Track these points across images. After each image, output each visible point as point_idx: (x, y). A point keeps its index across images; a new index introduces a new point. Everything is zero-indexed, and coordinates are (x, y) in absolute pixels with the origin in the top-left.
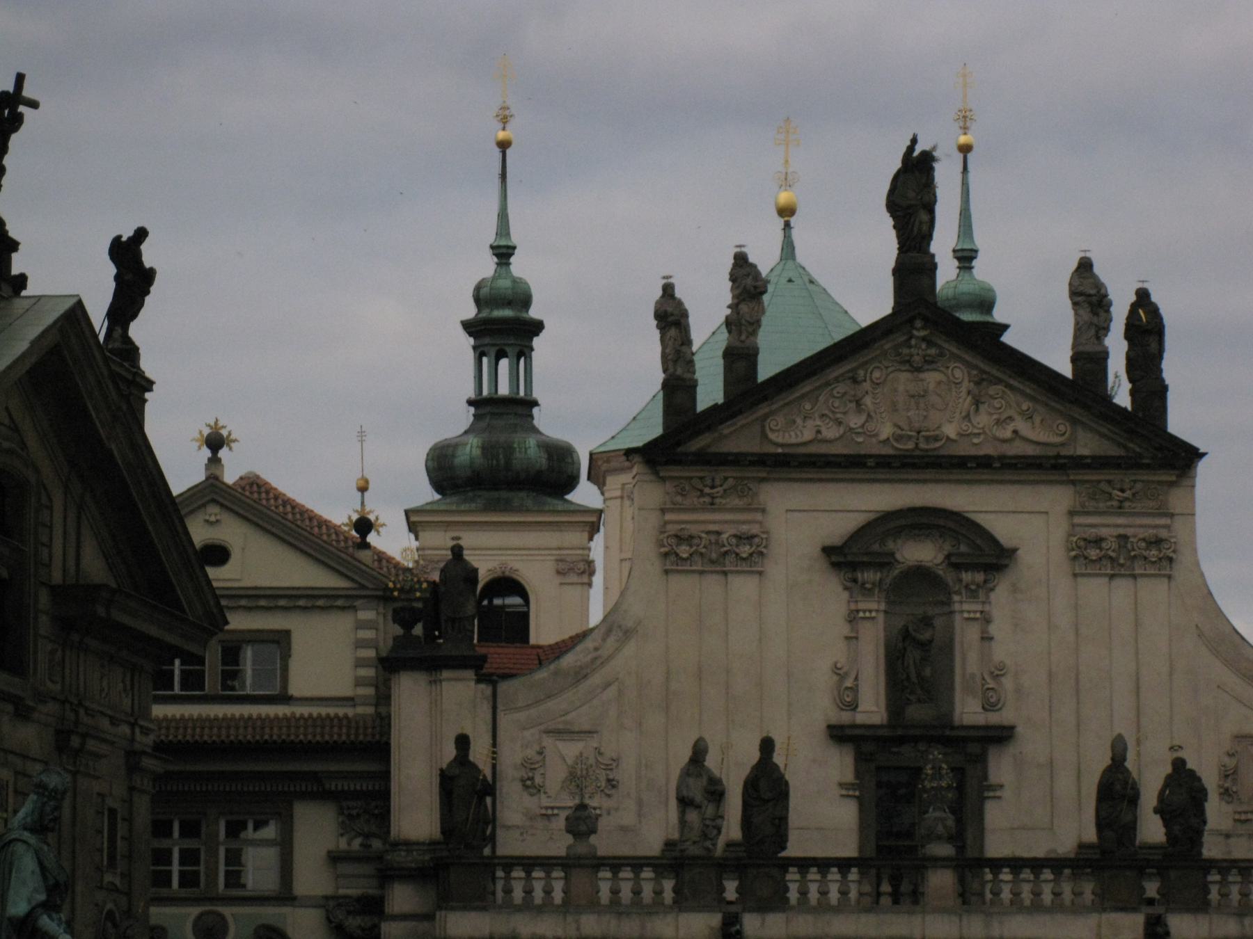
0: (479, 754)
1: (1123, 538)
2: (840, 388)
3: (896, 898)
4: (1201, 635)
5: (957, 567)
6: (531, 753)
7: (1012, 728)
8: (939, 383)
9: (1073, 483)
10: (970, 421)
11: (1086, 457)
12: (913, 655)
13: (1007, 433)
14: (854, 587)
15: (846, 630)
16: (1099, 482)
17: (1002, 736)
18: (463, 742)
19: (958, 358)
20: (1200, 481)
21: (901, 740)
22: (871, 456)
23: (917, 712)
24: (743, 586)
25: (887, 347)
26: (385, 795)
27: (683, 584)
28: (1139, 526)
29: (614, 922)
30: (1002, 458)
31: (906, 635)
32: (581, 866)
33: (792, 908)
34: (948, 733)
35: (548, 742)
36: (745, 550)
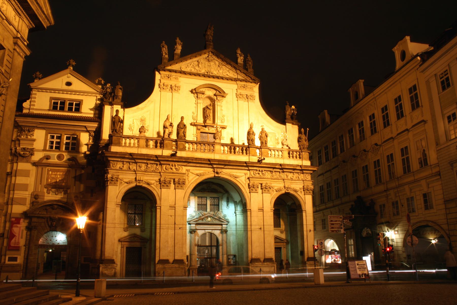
0: (121, 115)
2: (195, 63)
7: (227, 126)
8: (213, 64)
11: (240, 79)
12: (208, 111)
13: (225, 74)
17: (224, 128)
21: (205, 126)
22: (201, 74)
30: (225, 77)
31: (207, 107)
33: (187, 151)
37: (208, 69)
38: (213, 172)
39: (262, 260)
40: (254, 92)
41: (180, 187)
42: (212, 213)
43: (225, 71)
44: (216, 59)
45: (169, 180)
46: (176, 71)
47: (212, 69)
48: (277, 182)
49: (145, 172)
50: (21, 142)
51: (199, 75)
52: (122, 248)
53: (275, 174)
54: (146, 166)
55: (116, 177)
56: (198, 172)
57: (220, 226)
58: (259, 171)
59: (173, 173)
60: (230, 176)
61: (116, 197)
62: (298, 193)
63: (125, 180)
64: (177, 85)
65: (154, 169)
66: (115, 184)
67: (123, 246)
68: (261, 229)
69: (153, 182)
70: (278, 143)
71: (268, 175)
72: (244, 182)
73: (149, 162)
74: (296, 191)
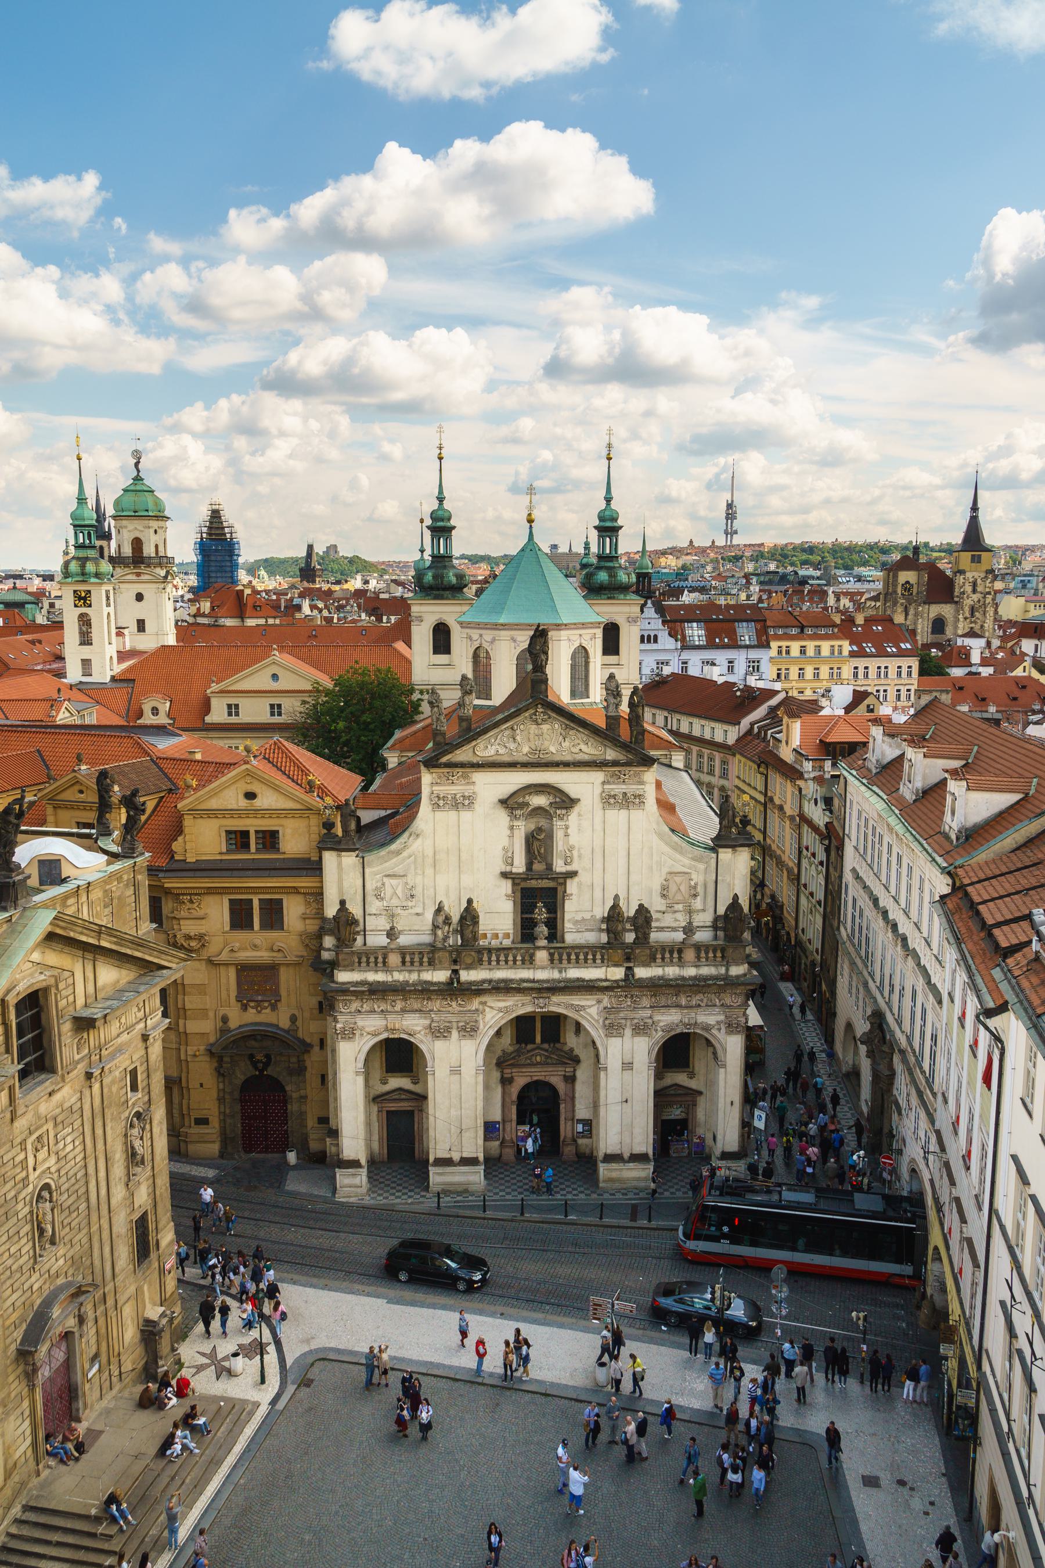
1: (625, 794)
2: (507, 733)
3: (523, 961)
6: (379, 884)
14: (513, 817)
15: (509, 832)
17: (573, 874)
18: (343, 903)
23: (538, 867)
24: (466, 815)
26: (322, 894)
27: (439, 815)
28: (631, 788)
29: (407, 975)
35: (385, 880)
36: (467, 802)
39: (626, 1156)
40: (642, 783)
42: (546, 1046)
43: (577, 741)
44: (553, 715)
46: (462, 765)
47: (546, 743)
50: (182, 922)
51: (512, 765)
56: (502, 1004)
62: (714, 1031)
63: (367, 1029)
64: (466, 794)
68: (626, 1101)
69: (419, 1028)
70: (695, 896)
71: (646, 1002)
72: (596, 1017)
74: (707, 1028)
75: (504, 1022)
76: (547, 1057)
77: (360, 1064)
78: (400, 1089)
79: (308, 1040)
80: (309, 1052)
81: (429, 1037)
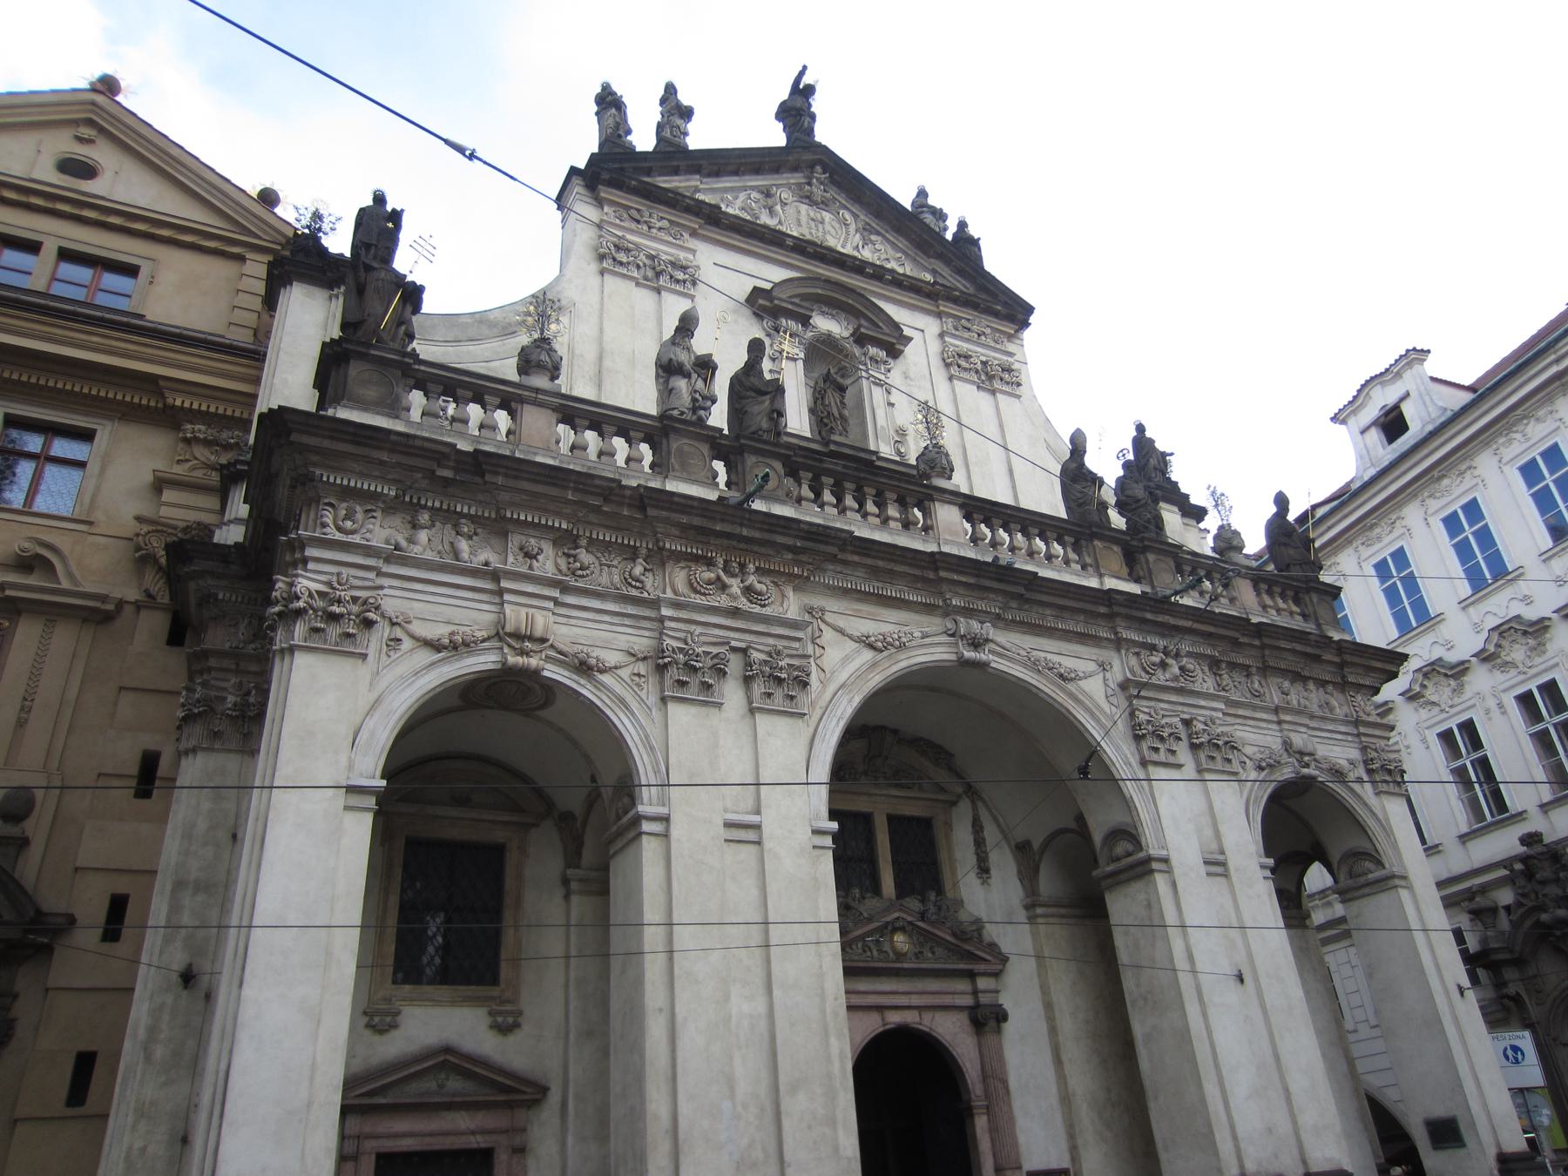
2: (754, 195)
4: (1048, 447)
5: (860, 339)
9: (939, 315)
10: (858, 251)
12: (832, 398)
16: (960, 318)
19: (846, 208)
20: (1025, 343)
25: (792, 181)
31: (827, 378)
32: (541, 405)
34: (874, 458)
36: (680, 275)
37: (814, 232)
38: (944, 638)
41: (778, 701)
42: (914, 904)
44: (842, 199)
45: (715, 650)
46: (672, 201)
48: (1251, 722)
49: (565, 589)
52: (350, 1166)
53: (1230, 681)
54: (568, 556)
55: (355, 599)
57: (963, 985)
58: (1166, 652)
59: (735, 613)
60: (1034, 665)
61: (345, 731)
63: (419, 629)
65: (616, 579)
66: (347, 648)
67: (350, 1148)
69: (612, 658)
73: (584, 532)
75: (876, 680)
76: (924, 938)
77: (369, 770)
78: (448, 1050)
79: (52, 901)
80: (48, 950)
81: (650, 693)
